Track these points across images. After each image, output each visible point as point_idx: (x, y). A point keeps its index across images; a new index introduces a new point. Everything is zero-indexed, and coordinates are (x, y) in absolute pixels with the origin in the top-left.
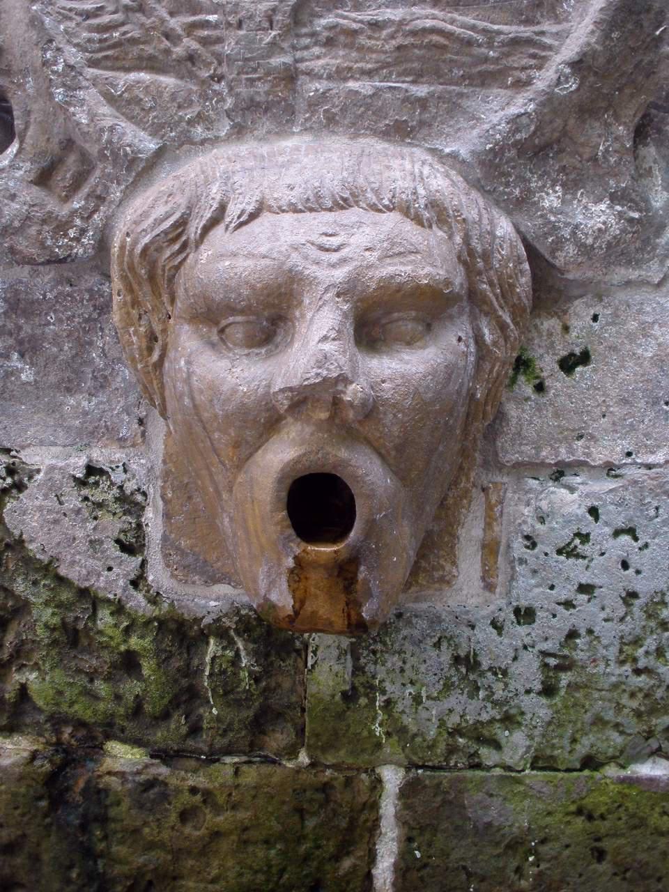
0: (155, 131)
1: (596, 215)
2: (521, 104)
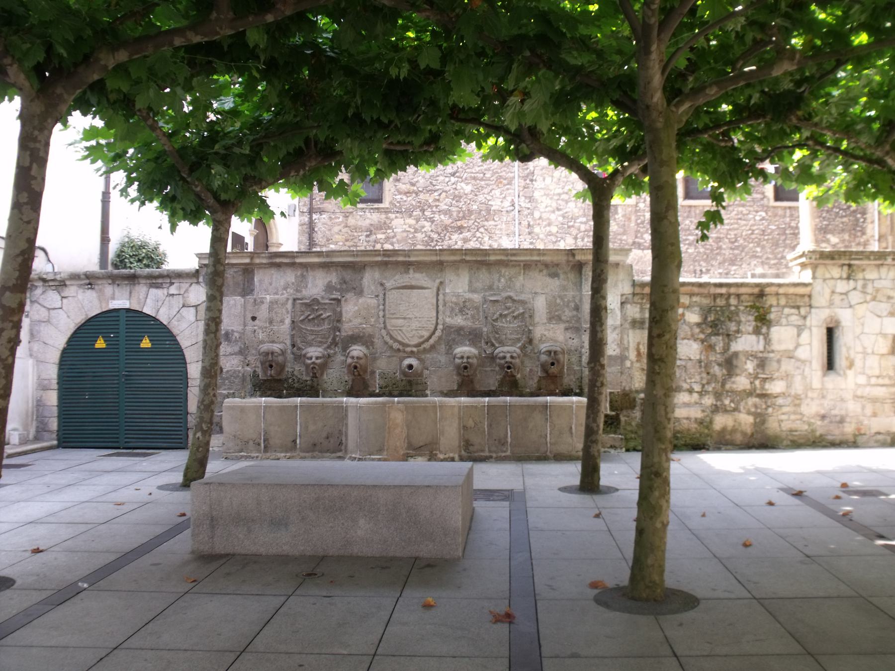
1: (332, 351)
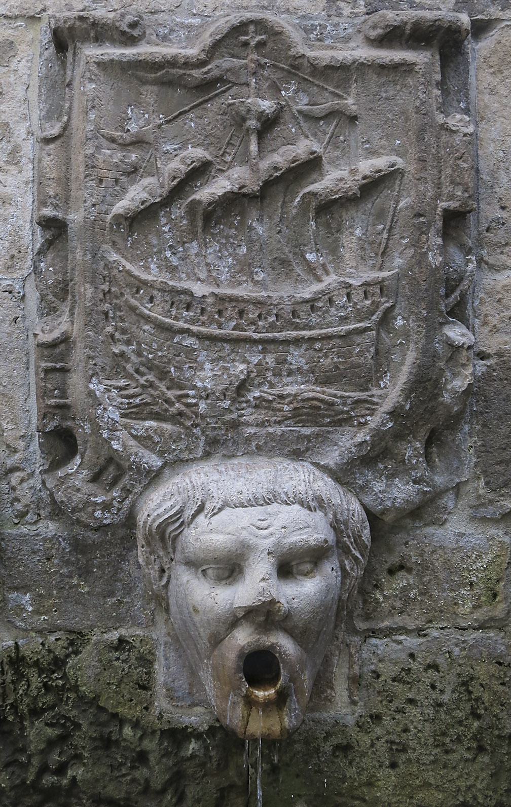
0: (161, 454)
2: (362, 436)
